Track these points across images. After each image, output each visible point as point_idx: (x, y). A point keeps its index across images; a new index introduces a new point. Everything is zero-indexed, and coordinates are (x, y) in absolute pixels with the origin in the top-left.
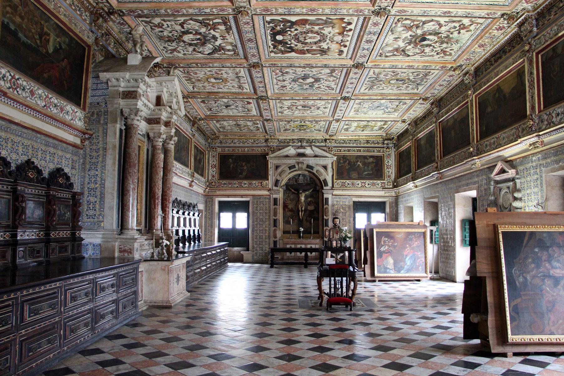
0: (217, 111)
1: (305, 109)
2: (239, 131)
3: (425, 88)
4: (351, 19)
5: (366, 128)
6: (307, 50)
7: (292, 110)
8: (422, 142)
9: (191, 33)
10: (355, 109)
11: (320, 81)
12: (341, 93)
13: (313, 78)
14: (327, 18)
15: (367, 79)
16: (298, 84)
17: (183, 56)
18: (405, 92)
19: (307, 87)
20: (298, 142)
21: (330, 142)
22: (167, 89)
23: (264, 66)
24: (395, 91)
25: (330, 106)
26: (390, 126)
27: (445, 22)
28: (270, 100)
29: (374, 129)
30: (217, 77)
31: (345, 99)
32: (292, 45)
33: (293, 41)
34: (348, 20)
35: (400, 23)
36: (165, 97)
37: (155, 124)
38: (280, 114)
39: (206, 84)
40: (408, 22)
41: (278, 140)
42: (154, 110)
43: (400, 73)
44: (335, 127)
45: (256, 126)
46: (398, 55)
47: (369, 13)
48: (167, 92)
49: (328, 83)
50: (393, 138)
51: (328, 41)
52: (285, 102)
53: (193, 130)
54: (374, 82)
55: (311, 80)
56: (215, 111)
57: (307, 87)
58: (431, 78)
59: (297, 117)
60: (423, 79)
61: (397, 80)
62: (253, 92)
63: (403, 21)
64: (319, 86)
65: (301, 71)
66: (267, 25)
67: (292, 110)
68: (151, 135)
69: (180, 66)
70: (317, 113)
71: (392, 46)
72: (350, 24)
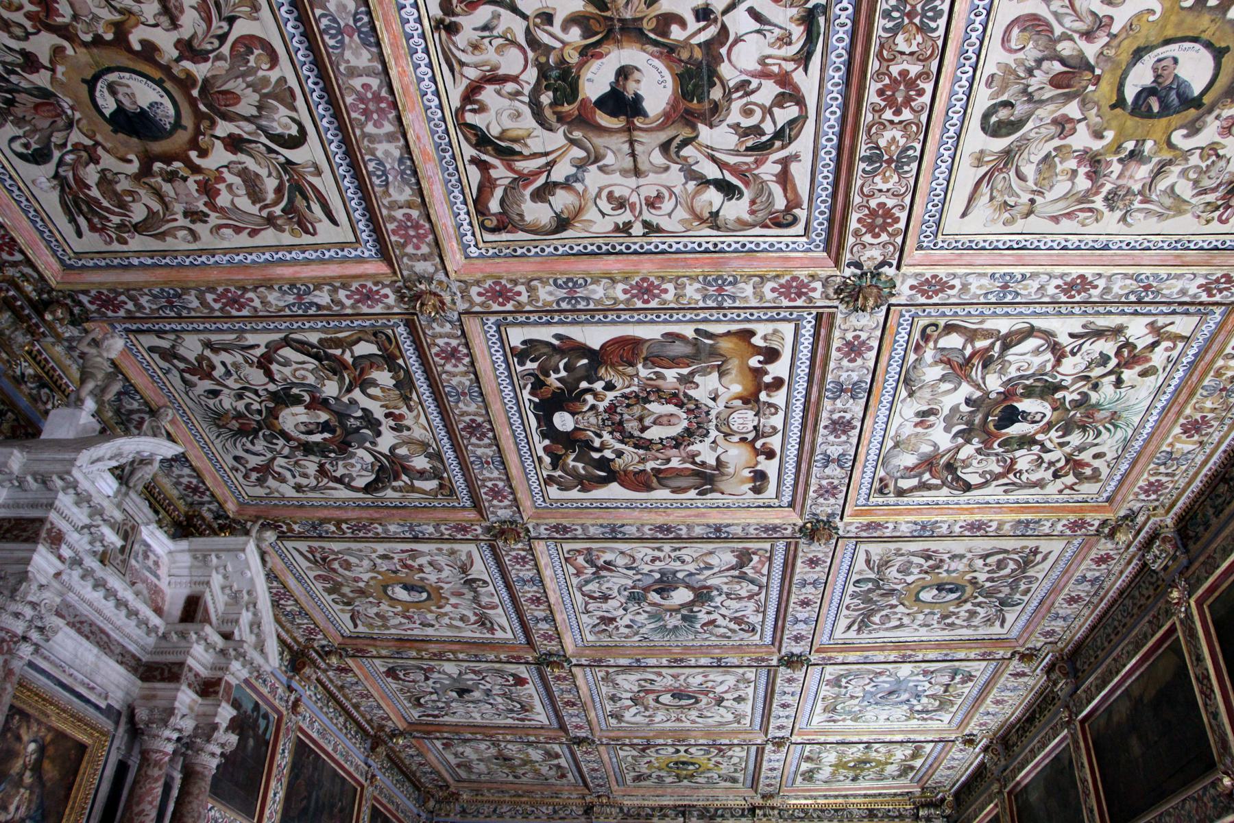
0: (438, 708)
1: (683, 702)
2: (511, 778)
3: (1024, 617)
4: (775, 332)
5: (862, 770)
6: (656, 471)
7: (646, 709)
8: (1034, 797)
9: (297, 400)
10: (827, 703)
11: (711, 599)
12: (777, 644)
13: (688, 586)
14: (697, 331)
15: (851, 589)
16: (648, 609)
17: (294, 494)
18: (966, 633)
19: (673, 621)
20: (677, 815)
21: (765, 815)
22: (225, 577)
23: (533, 534)
24: (940, 634)
25: (750, 691)
26: (930, 761)
27: (1072, 335)
28: (574, 669)
29: (886, 773)
30: (408, 581)
31: (791, 661)
32: (608, 454)
33: (607, 436)
34: (765, 338)
35: (931, 344)
36: (216, 602)
37: (163, 680)
38: (613, 721)
39: (384, 607)
40: (954, 341)
41: (621, 810)
42: (164, 637)
43: (945, 557)
44: (776, 765)
45: (555, 762)
46: (937, 487)
47: (827, 297)
48: (223, 588)
49: (734, 604)
50: (943, 800)
51: (714, 433)
52: (620, 679)
53: (370, 761)
54: (870, 601)
55: (682, 596)
56: (433, 708)
57: (673, 621)
58: (1041, 576)
59: (662, 733)
60: (1017, 581)
61: (940, 588)
62: (523, 641)
63: (939, 336)
64: (712, 617)
65: (648, 559)
66: (519, 369)
67: (646, 709)
68: (142, 714)
69: (292, 530)
70: (718, 719)
71: (914, 451)
72: (772, 355)
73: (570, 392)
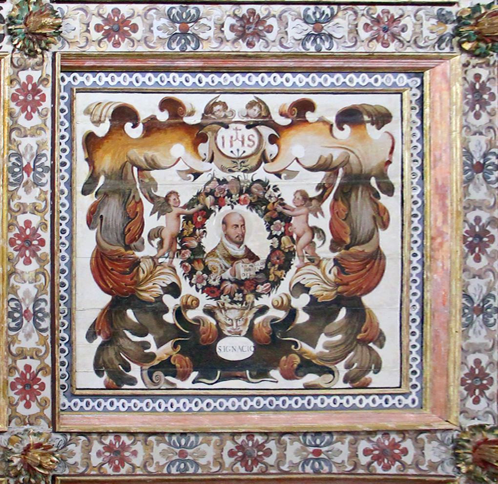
14: (85, 192)
32: (301, 302)
51: (260, 174)
66: (140, 384)
72: (124, 114)
73: (181, 334)
